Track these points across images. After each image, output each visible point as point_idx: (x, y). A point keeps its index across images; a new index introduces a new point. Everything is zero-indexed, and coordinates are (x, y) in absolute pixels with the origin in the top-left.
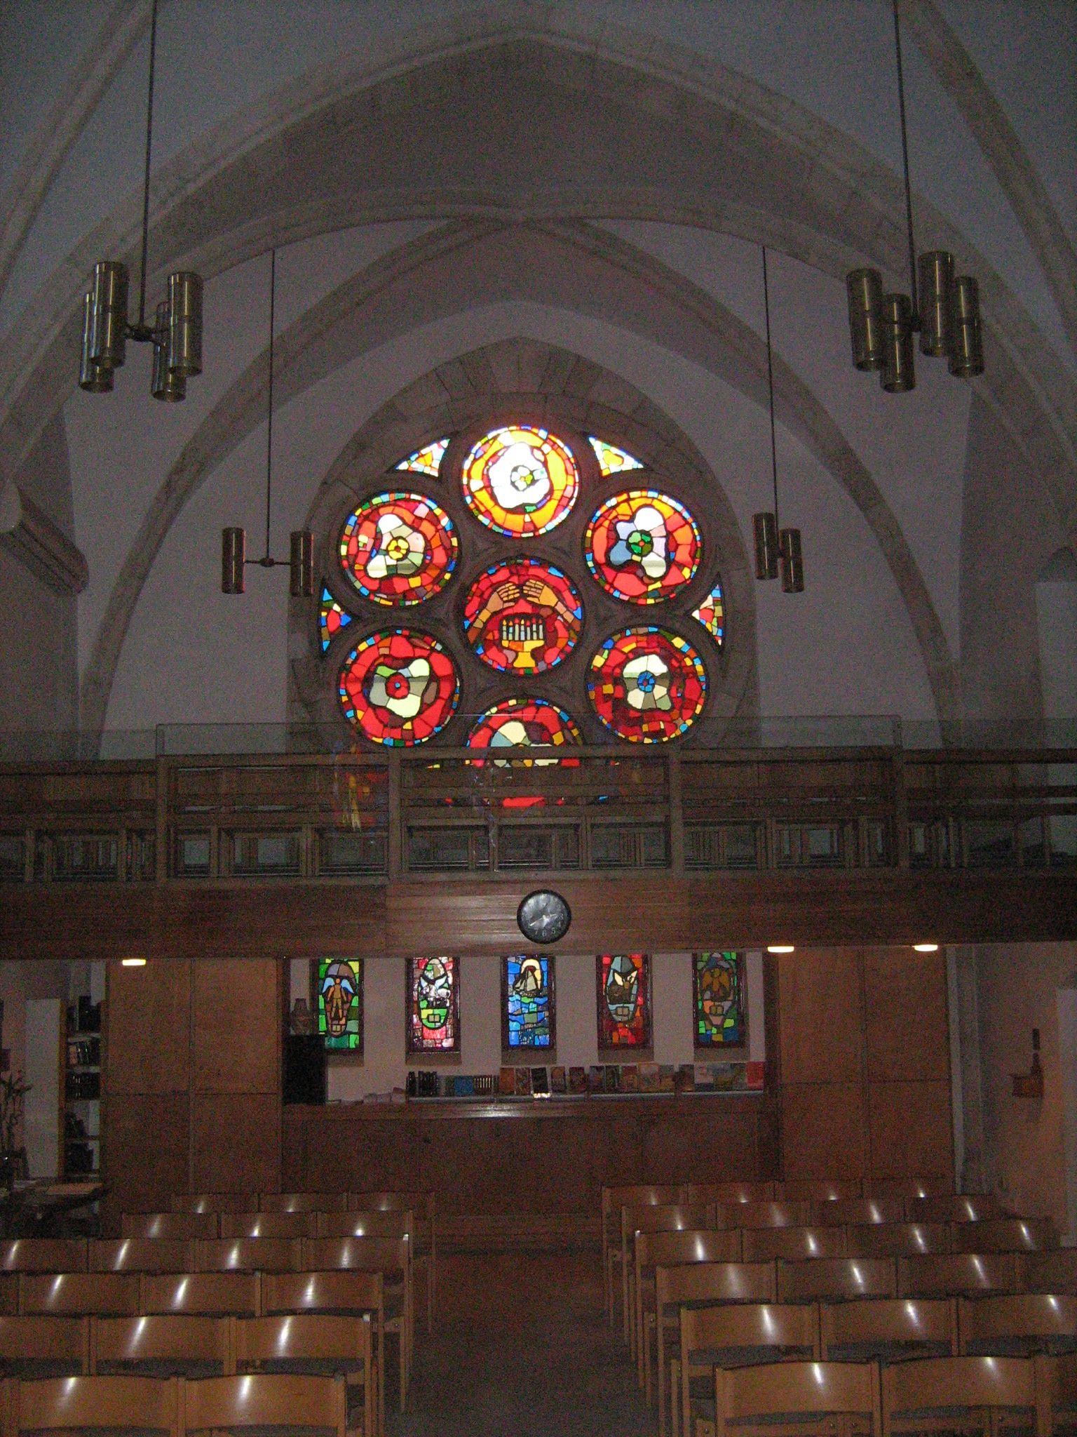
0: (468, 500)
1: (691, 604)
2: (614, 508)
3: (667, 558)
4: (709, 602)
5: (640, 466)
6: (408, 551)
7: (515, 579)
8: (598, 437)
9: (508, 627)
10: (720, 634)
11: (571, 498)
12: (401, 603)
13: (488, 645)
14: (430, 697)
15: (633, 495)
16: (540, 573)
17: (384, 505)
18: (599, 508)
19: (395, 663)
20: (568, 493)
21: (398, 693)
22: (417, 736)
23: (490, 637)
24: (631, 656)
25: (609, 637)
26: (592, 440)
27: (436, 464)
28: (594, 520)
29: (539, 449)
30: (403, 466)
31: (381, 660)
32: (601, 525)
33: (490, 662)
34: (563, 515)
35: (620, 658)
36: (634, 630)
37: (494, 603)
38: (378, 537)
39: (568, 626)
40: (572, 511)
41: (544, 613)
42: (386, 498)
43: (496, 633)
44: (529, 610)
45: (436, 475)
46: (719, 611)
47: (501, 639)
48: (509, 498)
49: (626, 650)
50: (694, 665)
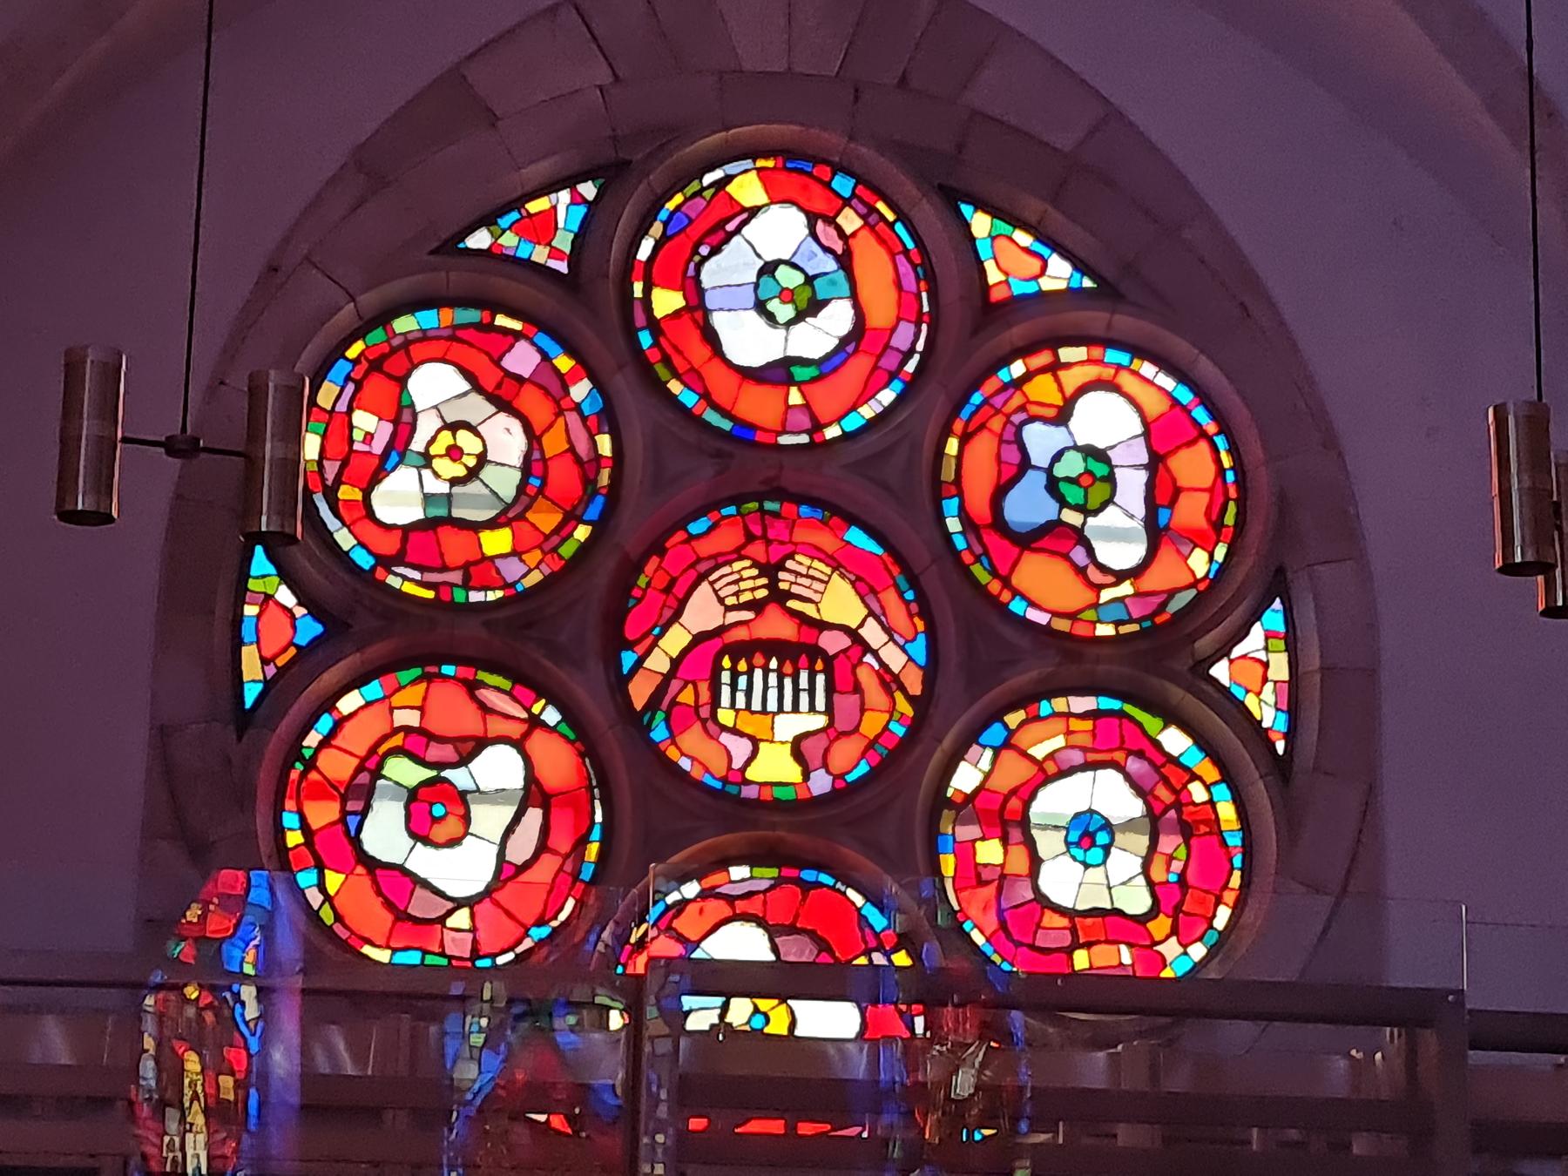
0: (645, 339)
1: (1205, 644)
2: (1018, 384)
3: (1151, 522)
4: (1254, 642)
5: (1087, 283)
6: (482, 459)
7: (758, 550)
8: (980, 206)
9: (735, 675)
10: (1281, 724)
11: (911, 351)
12: (459, 595)
13: (679, 721)
14: (522, 848)
15: (1067, 354)
16: (826, 541)
17: (424, 336)
18: (976, 386)
19: (435, 752)
20: (901, 339)
21: (439, 833)
22: (484, 949)
23: (687, 697)
24: (1051, 768)
25: (997, 716)
26: (966, 210)
27: (563, 242)
28: (966, 413)
29: (831, 221)
30: (480, 240)
31: (397, 740)
32: (982, 427)
33: (685, 764)
34: (887, 396)
35: (1024, 772)
36: (1060, 704)
37: (702, 612)
38: (403, 421)
39: (889, 681)
40: (912, 386)
41: (832, 643)
42: (428, 319)
43: (704, 687)
44: (786, 630)
45: (562, 267)
46: (1280, 668)
47: (715, 703)
48: (747, 340)
49: (1039, 752)
50: (1211, 803)
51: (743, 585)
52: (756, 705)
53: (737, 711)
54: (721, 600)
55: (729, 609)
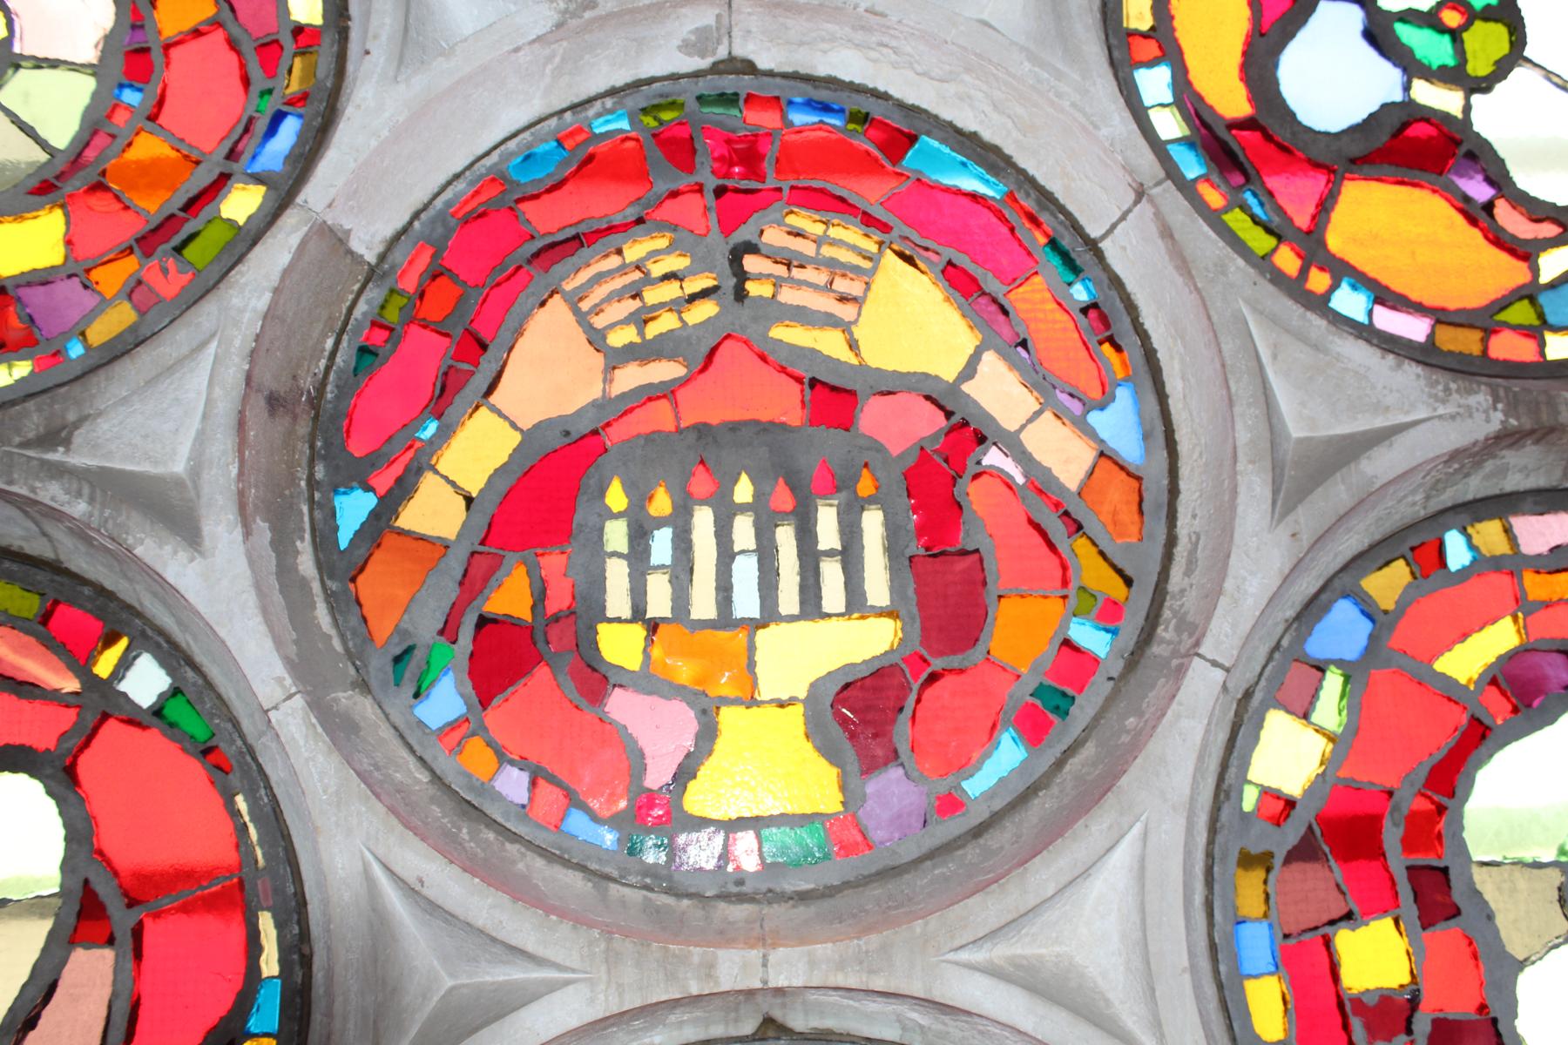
51: (652, 296)
52: (703, 605)
53: (653, 626)
54: (596, 339)
55: (616, 359)
